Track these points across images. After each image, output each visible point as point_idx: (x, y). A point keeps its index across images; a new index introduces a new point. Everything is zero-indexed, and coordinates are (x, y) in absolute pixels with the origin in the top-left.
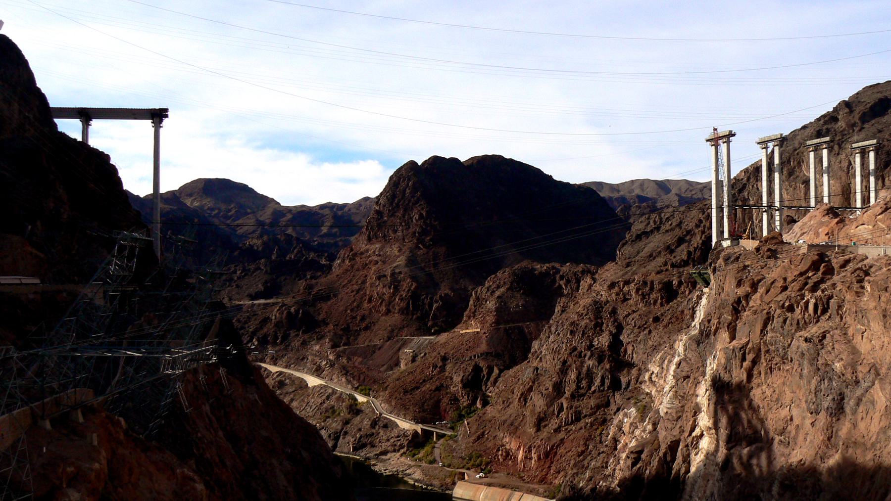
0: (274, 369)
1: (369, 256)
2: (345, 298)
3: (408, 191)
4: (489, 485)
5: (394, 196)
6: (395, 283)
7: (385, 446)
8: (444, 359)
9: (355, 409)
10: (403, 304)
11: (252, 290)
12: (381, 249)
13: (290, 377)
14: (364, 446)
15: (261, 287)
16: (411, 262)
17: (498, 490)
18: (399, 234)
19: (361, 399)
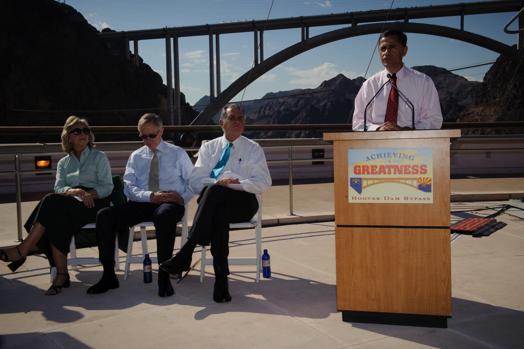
1: (474, 116)
3: (507, 68)
12: (483, 111)
18: (498, 100)
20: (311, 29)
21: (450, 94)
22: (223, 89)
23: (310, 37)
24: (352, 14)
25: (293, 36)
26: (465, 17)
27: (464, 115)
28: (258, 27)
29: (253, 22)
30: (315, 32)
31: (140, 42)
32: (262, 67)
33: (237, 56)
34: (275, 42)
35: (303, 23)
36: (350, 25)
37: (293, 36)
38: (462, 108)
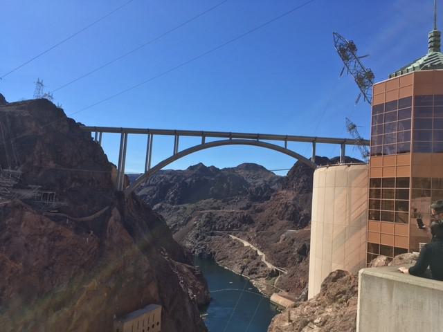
0: (234, 237)
2: (268, 211)
4: (284, 297)
5: (294, 171)
6: (287, 207)
7: (260, 274)
8: (293, 240)
9: (255, 256)
10: (289, 216)
11: (242, 207)
13: (238, 241)
14: (252, 274)
15: (245, 206)
16: (295, 199)
17: (286, 299)
19: (260, 253)
20: (206, 138)
21: (265, 181)
22: (151, 167)
23: (206, 142)
24: (230, 133)
25: (197, 141)
26: (288, 142)
27: (276, 195)
28: (177, 133)
29: (175, 131)
30: (208, 140)
31: (103, 134)
32: (177, 156)
33: (163, 149)
34: (186, 143)
35: (203, 134)
36: (228, 139)
37: (197, 141)
38: (273, 191)
